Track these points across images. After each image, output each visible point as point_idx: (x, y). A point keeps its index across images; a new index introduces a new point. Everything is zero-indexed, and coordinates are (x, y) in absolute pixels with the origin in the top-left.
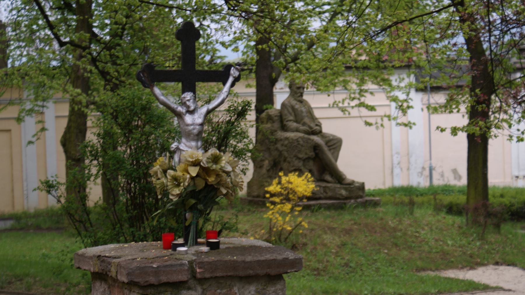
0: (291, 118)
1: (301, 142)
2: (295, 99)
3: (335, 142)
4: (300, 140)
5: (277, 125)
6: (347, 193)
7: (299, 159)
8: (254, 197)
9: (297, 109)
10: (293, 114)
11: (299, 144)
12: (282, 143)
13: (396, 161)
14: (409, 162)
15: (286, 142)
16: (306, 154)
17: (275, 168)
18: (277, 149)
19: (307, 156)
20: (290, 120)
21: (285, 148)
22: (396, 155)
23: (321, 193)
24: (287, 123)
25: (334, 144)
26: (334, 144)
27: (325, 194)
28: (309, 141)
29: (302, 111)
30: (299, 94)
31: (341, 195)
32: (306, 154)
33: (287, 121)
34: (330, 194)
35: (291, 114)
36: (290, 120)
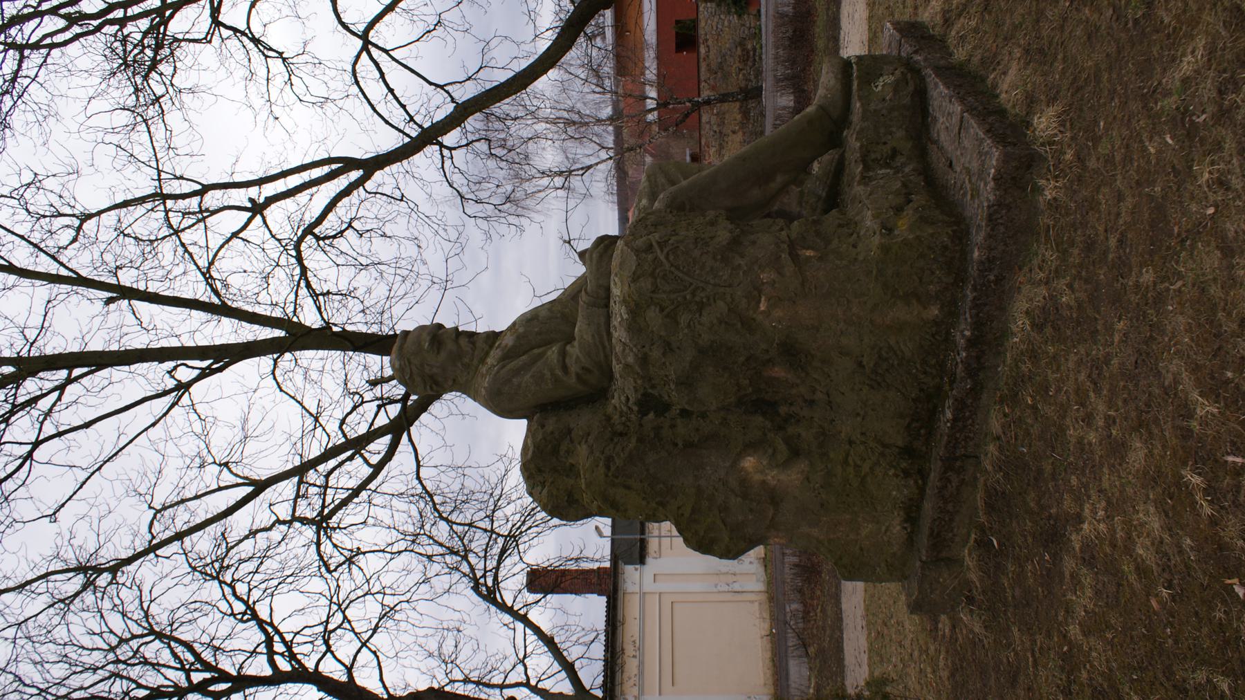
0: (553, 353)
1: (655, 238)
2: (482, 361)
5: (582, 420)
8: (910, 541)
10: (536, 351)
11: (662, 245)
12: (656, 353)
13: (726, 588)
14: (727, 573)
15: (653, 317)
16: (713, 223)
17: (783, 410)
18: (686, 383)
20: (563, 354)
21: (684, 319)
22: (719, 587)
24: (573, 369)
33: (565, 368)
34: (898, 137)
35: (541, 356)
36: (563, 354)
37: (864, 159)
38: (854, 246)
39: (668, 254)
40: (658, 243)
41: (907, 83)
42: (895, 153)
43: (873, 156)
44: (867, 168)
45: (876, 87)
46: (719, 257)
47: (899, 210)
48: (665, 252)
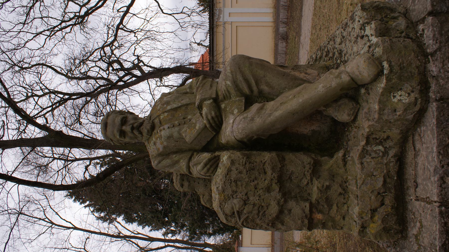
1: (236, 203)
3: (240, 78)
4: (228, 208)
6: (407, 87)
7: (281, 212)
9: (164, 147)
10: (175, 157)
11: (239, 213)
16: (268, 189)
19: (276, 188)
23: (385, 153)
25: (247, 81)
26: (247, 81)
27: (389, 143)
28: (234, 175)
29: (170, 137)
30: (136, 132)
31: (407, 108)
32: (268, 189)
34: (395, 133)
35: (177, 162)
37: (368, 138)
38: (344, 218)
39: (243, 222)
40: (238, 212)
41: (416, 105)
42: (388, 137)
43: (374, 136)
44: (368, 143)
45: (394, 97)
46: (270, 224)
47: (374, 211)
48: (242, 220)
